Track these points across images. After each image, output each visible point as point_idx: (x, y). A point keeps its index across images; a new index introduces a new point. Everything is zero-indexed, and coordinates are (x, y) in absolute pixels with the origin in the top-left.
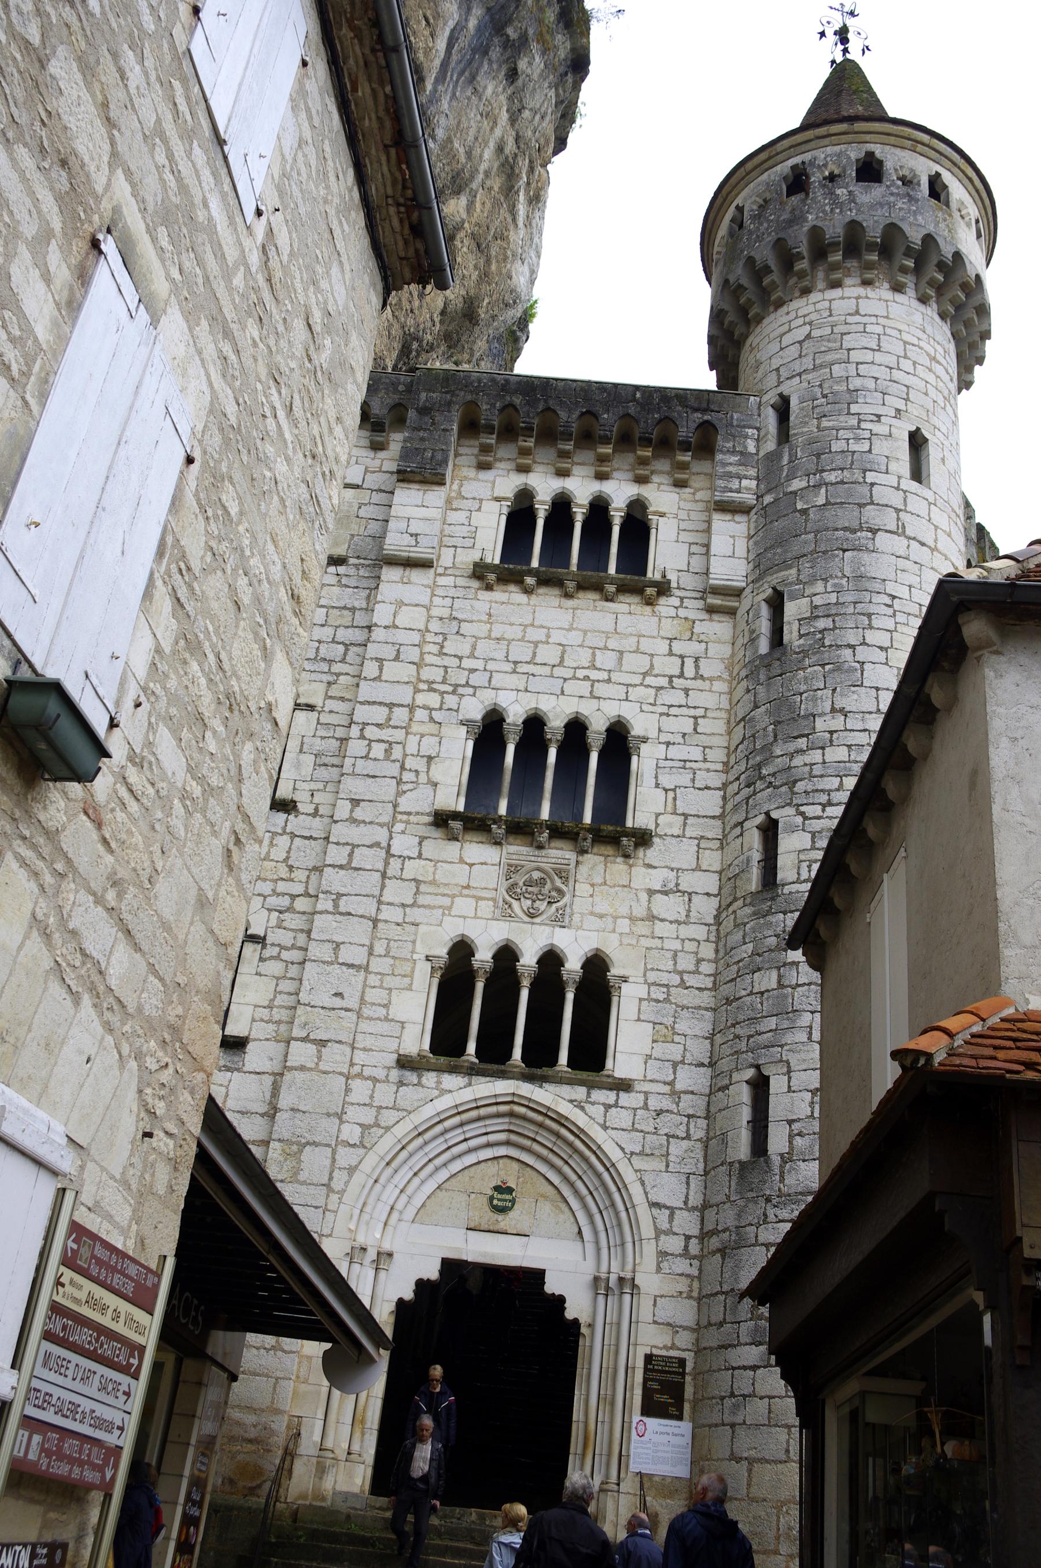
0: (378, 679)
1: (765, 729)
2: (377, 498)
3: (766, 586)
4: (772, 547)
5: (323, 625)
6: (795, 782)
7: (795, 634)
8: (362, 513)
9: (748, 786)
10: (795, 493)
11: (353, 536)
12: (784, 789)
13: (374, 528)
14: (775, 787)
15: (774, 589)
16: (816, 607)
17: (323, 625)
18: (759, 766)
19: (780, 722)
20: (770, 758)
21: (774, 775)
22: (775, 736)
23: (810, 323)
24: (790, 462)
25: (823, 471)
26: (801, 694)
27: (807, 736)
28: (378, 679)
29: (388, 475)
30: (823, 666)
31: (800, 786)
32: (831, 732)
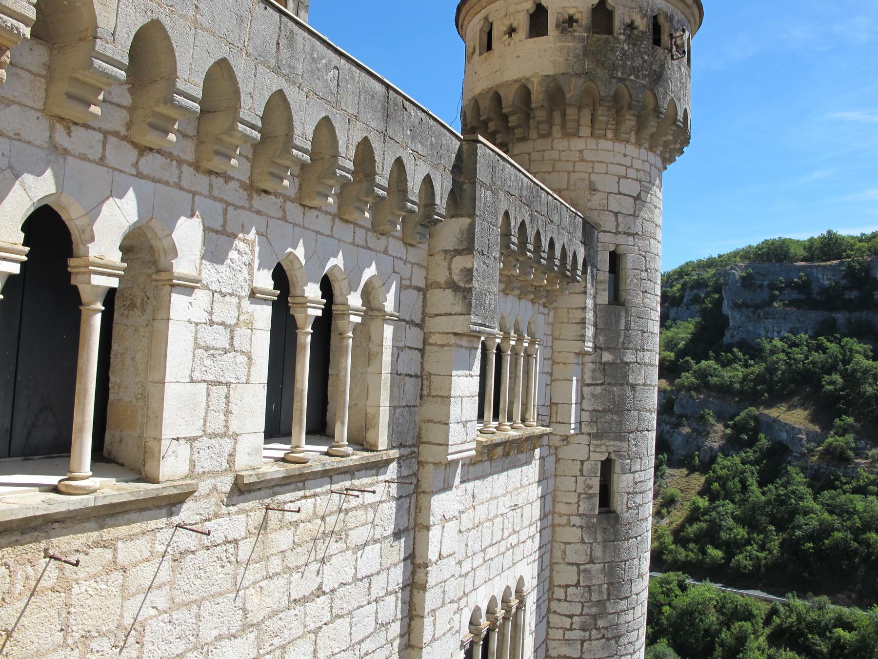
0: (434, 639)
1: (600, 586)
3: (603, 449)
4: (610, 411)
5: (378, 573)
6: (619, 637)
7: (625, 506)
9: (584, 630)
10: (628, 364)
12: (613, 642)
14: (608, 639)
15: (609, 453)
16: (636, 483)
17: (378, 573)
18: (595, 617)
19: (612, 584)
20: (603, 614)
21: (606, 628)
22: (609, 595)
23: (640, 181)
24: (626, 329)
25: (644, 350)
26: (625, 561)
27: (626, 598)
28: (434, 639)
29: (416, 292)
30: (636, 538)
31: (623, 640)
32: (637, 594)
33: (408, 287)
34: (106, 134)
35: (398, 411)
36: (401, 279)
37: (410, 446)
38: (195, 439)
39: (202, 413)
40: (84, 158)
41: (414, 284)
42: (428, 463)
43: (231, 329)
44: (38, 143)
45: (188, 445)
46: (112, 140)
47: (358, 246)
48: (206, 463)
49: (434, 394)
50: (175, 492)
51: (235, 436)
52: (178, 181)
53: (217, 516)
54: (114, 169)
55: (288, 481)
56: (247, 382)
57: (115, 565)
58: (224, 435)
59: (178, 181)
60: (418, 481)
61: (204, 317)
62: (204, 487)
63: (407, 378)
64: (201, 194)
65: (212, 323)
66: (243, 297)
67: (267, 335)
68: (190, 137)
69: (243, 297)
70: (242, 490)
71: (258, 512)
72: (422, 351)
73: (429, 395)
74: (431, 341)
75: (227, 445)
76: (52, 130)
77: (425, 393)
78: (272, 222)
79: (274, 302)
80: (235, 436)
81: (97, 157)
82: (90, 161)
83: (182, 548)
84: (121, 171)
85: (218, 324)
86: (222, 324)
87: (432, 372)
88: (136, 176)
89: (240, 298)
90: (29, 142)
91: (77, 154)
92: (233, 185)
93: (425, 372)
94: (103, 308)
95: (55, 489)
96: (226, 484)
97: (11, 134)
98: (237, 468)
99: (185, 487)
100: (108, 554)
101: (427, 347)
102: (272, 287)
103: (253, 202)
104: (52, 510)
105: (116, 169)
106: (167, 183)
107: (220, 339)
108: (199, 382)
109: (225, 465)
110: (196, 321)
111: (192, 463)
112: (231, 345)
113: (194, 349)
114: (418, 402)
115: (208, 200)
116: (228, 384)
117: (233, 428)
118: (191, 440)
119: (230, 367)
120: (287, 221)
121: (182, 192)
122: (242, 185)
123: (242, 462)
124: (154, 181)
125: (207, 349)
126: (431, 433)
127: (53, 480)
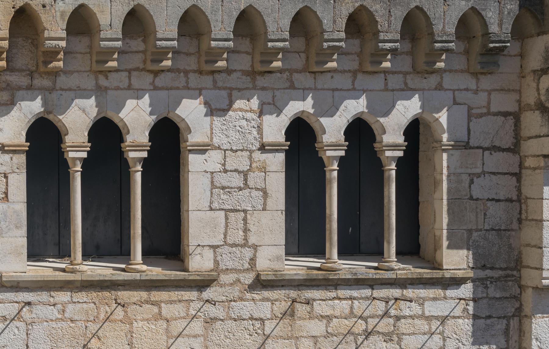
2: (494, 161)
8: (476, 194)
11: (470, 231)
13: (497, 214)
33: (481, 116)
34: (129, 71)
35: (475, 234)
36: (470, 109)
37: (501, 269)
38: (218, 247)
39: (223, 230)
40: (117, 88)
41: (493, 109)
42: (528, 287)
43: (245, 174)
44: (90, 88)
45: (212, 251)
46: (134, 73)
47: (393, 90)
48: (227, 262)
49: (530, 218)
50: (198, 278)
51: (255, 247)
52: (185, 85)
53: (241, 299)
54: (138, 90)
55: (314, 283)
56: (264, 209)
57: (159, 316)
58: (243, 246)
59: (185, 85)
60: (521, 305)
61: (219, 167)
62: (225, 278)
63: (489, 204)
64: (206, 89)
65: (226, 171)
66: (253, 151)
67: (282, 176)
68: (193, 54)
69: (253, 151)
70: (261, 284)
71: (283, 303)
72: (518, 176)
73: (526, 219)
74: (527, 164)
75: (248, 253)
76: (97, 79)
77: (523, 217)
78: (277, 93)
79: (286, 151)
80: (255, 247)
81: (126, 85)
82: (121, 89)
83: (212, 316)
84: (142, 90)
85: (231, 171)
86: (236, 170)
87: (528, 196)
88: (154, 90)
89: (251, 152)
90: (85, 90)
91: (113, 88)
92: (234, 75)
93: (523, 197)
94: (142, 169)
95: (123, 270)
96: (248, 278)
97: (75, 88)
98: (258, 269)
99: (206, 276)
100: (156, 310)
101: (523, 171)
102: (284, 140)
103: (256, 82)
104: (114, 278)
105: (140, 89)
106: (178, 88)
107: (237, 181)
108: (217, 210)
109: (247, 266)
110: (211, 171)
111: (216, 262)
112: (246, 184)
113: (212, 189)
114: (515, 225)
115: (213, 91)
116: (245, 211)
117: (252, 240)
118: (214, 247)
119: (249, 200)
120: (295, 88)
121: (190, 91)
122: (245, 73)
123: (264, 263)
124: (167, 89)
125: (223, 188)
126: (529, 257)
127: (123, 266)
